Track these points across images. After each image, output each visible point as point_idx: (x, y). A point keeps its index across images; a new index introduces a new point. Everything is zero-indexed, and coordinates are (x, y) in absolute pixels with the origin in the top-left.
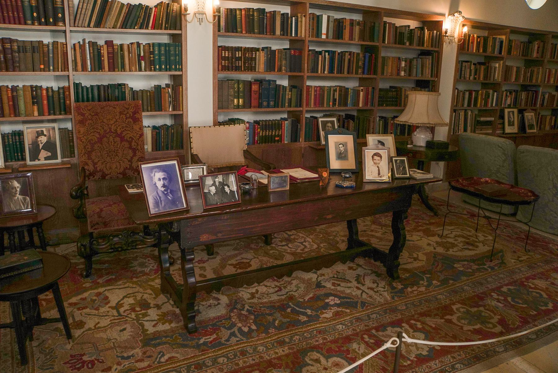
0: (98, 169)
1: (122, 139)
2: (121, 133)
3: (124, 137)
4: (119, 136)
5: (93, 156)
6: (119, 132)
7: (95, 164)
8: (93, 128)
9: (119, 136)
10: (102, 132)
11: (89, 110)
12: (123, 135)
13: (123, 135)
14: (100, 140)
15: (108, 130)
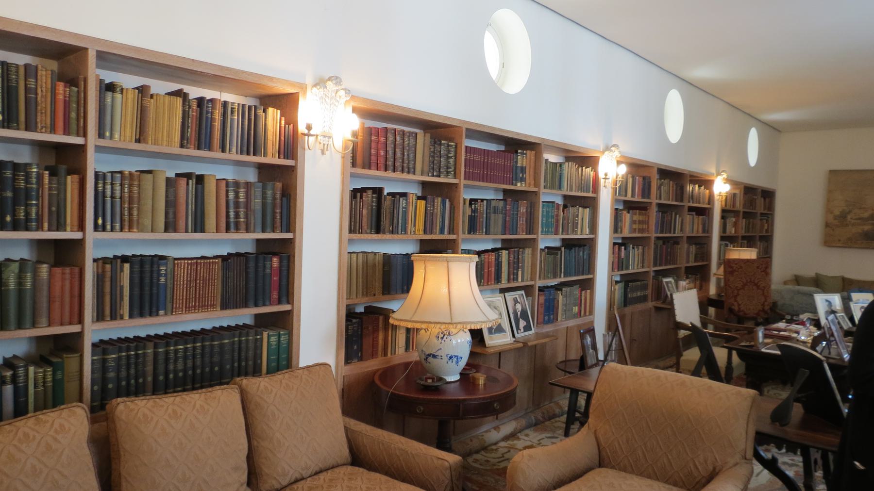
0: (742, 309)
1: (758, 287)
2: (758, 283)
3: (759, 286)
4: (756, 285)
5: (739, 299)
6: (756, 282)
7: (739, 305)
8: (739, 278)
9: (756, 285)
10: (745, 282)
11: (736, 264)
12: (759, 284)
13: (759, 284)
14: (743, 287)
15: (749, 281)
